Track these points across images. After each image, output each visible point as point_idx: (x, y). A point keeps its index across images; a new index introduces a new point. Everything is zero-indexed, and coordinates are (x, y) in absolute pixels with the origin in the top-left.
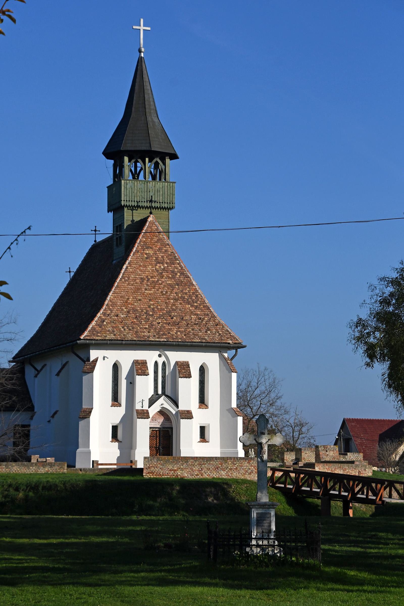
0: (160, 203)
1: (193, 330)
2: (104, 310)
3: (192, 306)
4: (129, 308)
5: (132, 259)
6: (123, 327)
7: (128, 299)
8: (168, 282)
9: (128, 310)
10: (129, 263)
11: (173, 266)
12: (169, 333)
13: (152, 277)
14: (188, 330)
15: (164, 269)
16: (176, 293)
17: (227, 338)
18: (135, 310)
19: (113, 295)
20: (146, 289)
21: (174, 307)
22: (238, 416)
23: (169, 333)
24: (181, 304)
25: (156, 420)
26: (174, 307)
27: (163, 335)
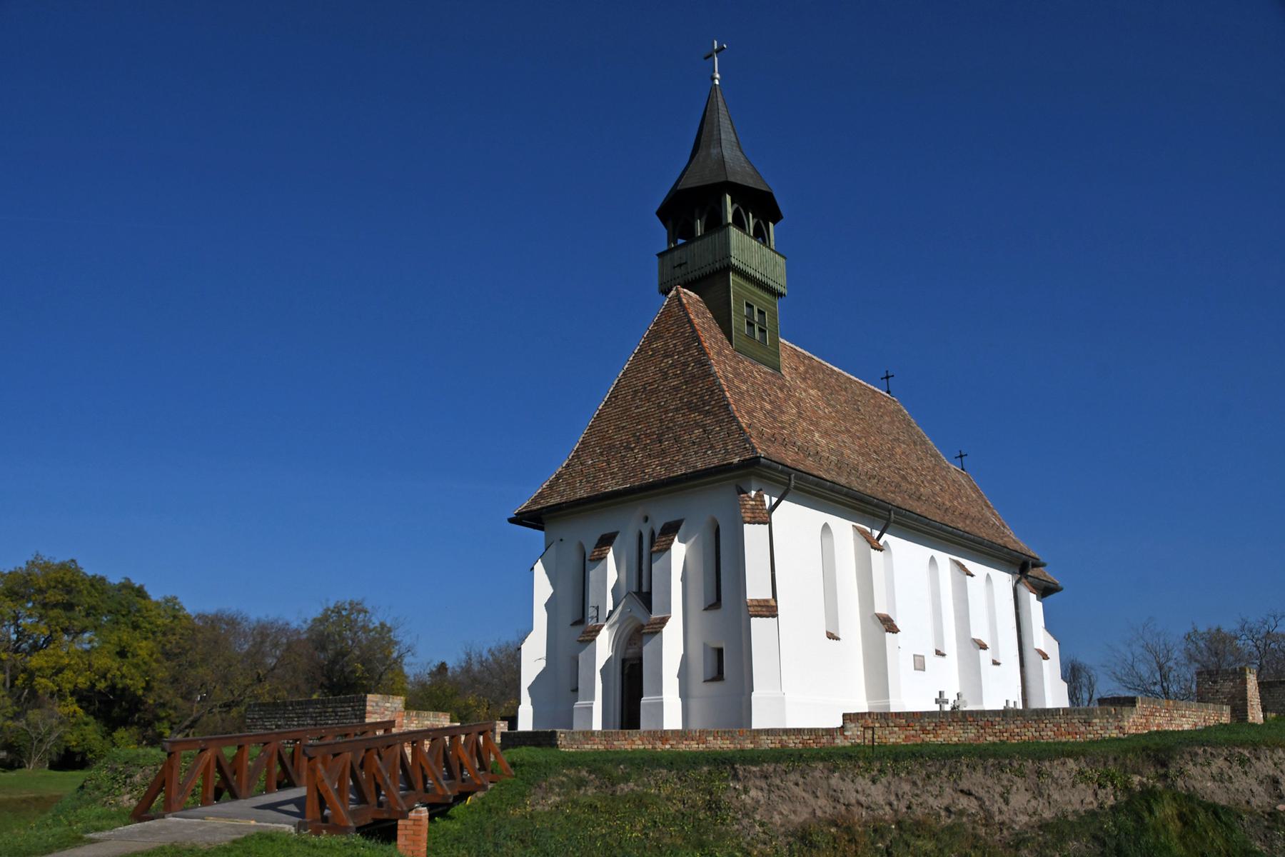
0: (709, 265)
1: (684, 456)
2: (570, 460)
4: (604, 447)
6: (581, 482)
8: (672, 384)
9: (602, 450)
10: (624, 374)
11: (687, 353)
12: (643, 472)
13: (651, 384)
14: (677, 458)
15: (671, 365)
17: (736, 454)
18: (611, 447)
19: (589, 431)
20: (637, 407)
21: (671, 425)
23: (643, 472)
24: (684, 415)
25: (635, 644)
26: (671, 425)
27: (631, 477)
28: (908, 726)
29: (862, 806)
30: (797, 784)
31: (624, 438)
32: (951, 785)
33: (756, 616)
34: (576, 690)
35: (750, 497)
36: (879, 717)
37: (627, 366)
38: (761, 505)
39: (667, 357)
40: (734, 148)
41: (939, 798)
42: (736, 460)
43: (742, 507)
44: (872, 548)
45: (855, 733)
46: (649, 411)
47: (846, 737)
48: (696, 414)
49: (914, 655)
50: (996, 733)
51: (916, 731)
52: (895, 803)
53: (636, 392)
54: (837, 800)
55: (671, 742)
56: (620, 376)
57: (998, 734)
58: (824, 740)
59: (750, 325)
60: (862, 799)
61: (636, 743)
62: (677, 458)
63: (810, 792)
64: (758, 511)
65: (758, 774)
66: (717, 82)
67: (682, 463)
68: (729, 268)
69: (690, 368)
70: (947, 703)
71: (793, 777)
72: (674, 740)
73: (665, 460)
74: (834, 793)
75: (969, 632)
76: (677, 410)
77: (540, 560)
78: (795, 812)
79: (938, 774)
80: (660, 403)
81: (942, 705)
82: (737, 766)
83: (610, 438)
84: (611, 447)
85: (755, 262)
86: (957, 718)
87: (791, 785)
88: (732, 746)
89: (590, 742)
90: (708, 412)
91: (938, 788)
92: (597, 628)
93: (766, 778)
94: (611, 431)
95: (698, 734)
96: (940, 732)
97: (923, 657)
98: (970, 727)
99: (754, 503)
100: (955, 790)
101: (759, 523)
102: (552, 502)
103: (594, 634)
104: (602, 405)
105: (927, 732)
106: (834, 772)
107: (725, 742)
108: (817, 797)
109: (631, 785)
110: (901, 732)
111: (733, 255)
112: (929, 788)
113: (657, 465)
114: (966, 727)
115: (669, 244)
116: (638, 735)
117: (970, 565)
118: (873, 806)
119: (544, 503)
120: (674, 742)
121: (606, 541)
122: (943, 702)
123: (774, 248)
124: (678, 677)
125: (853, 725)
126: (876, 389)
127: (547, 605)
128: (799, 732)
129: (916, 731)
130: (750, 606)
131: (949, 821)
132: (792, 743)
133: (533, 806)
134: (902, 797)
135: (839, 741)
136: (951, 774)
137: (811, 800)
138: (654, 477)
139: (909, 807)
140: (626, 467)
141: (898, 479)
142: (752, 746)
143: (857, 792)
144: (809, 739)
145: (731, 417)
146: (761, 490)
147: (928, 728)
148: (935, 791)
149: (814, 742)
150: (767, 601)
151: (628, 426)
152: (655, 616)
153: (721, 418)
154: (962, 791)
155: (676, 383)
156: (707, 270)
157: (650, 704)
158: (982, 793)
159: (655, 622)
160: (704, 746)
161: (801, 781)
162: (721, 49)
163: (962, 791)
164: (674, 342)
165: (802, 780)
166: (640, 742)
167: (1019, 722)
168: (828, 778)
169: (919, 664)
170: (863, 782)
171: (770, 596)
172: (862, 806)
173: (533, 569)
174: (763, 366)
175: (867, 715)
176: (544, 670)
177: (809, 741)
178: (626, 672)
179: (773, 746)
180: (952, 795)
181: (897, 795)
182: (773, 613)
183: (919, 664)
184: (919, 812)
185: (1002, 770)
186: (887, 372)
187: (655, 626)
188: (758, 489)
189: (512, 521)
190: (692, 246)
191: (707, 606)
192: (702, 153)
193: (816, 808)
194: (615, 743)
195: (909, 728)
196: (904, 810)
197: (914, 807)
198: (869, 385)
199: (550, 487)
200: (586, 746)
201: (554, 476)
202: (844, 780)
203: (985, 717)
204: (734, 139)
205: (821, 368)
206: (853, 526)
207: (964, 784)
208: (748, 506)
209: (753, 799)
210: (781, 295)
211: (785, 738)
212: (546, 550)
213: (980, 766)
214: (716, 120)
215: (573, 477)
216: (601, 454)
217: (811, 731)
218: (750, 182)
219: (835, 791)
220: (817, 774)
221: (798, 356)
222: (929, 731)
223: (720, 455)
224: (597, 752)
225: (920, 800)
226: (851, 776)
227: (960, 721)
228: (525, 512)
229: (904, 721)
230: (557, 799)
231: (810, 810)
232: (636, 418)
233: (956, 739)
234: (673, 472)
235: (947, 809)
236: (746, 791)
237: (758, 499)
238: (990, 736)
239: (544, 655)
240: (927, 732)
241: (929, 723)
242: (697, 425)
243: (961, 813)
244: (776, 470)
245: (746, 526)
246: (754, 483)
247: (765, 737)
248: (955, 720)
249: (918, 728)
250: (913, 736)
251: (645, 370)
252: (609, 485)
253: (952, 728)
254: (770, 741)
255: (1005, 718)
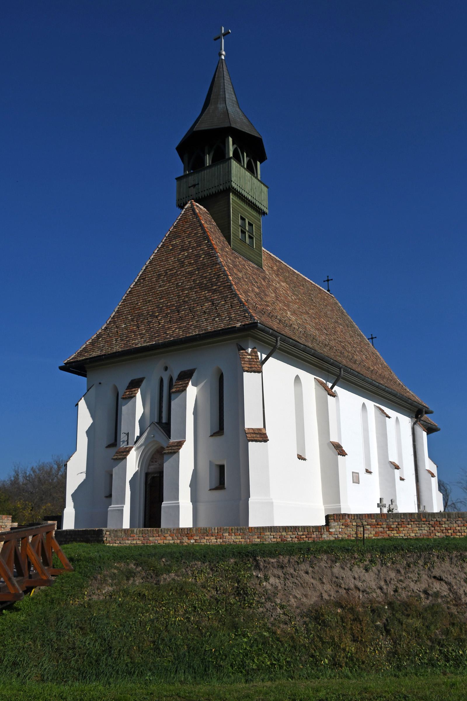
1: (197, 321)
3: (209, 291)
4: (134, 315)
5: (155, 257)
6: (116, 340)
7: (137, 303)
8: (188, 270)
9: (133, 317)
10: (150, 263)
11: (200, 248)
12: (165, 333)
13: (171, 270)
14: (192, 323)
15: (186, 257)
16: (194, 281)
17: (238, 321)
19: (123, 303)
20: (160, 287)
21: (187, 299)
22: (249, 441)
23: (165, 333)
24: (196, 292)
25: (156, 462)
26: (187, 299)
27: (156, 337)
28: (378, 525)
29: (359, 590)
30: (307, 573)
31: (150, 308)
32: (426, 573)
33: (252, 441)
34: (110, 496)
35: (247, 353)
36: (356, 518)
37: (152, 257)
38: (256, 359)
39: (184, 250)
40: (235, 105)
41: (418, 583)
42: (238, 325)
43: (242, 359)
44: (329, 394)
45: (338, 530)
46: (170, 289)
47: (331, 533)
48: (206, 292)
49: (353, 472)
50: (443, 530)
51: (383, 528)
52: (385, 587)
53: (160, 275)
54: (339, 586)
55: (195, 538)
56: (147, 264)
57: (444, 531)
58: (314, 536)
59: (243, 232)
60: (359, 584)
61: (168, 538)
62: (192, 323)
63: (317, 579)
64: (253, 363)
65: (275, 566)
66: (223, 57)
67: (196, 327)
68: (230, 189)
69: (201, 259)
70: (385, 506)
71: (304, 567)
72: (197, 536)
73: (182, 325)
74: (336, 580)
75: (387, 457)
76: (191, 289)
77: (83, 398)
78: (306, 596)
79: (415, 563)
80: (178, 283)
81: (382, 508)
82: (258, 558)
83: (139, 309)
84: (140, 315)
85: (248, 188)
86: (414, 518)
87: (302, 573)
88: (243, 540)
89: (130, 538)
90: (215, 290)
91: (417, 575)
92: (127, 449)
93: (282, 567)
94: (140, 304)
95: (216, 531)
96: (401, 529)
97: (358, 473)
98: (423, 526)
99: (250, 357)
100: (430, 577)
101: (255, 372)
102: (94, 354)
103: (125, 453)
104: (133, 284)
105: (392, 529)
106: (336, 562)
107: (237, 537)
108: (323, 583)
109: (173, 575)
110: (372, 529)
111: (233, 180)
112: (410, 575)
113: (176, 329)
114: (420, 526)
115: (185, 171)
116: (169, 533)
117: (388, 411)
118: (368, 590)
119: (87, 356)
120: (198, 538)
121: (135, 384)
122: (383, 506)
123: (260, 179)
124: (190, 486)
125: (336, 524)
126: (321, 288)
127: (88, 432)
128: (295, 528)
129: (383, 528)
130: (248, 433)
131: (428, 602)
132: (289, 537)
133: (90, 596)
134: (390, 582)
135: (326, 536)
136: (425, 564)
137: (319, 586)
138: (174, 337)
139: (396, 591)
140: (152, 330)
141: (341, 349)
142: (259, 540)
143: (355, 578)
144: (303, 535)
145: (233, 294)
146: (255, 348)
147: (392, 526)
148: (415, 577)
149: (306, 537)
150: (260, 429)
151: (153, 300)
152: (173, 440)
153: (225, 295)
154: (435, 577)
155: (190, 269)
156: (214, 191)
157: (168, 507)
158: (450, 579)
159: (174, 445)
160: (221, 540)
161: (310, 570)
162: (227, 34)
163: (435, 577)
164: (189, 240)
165: (311, 569)
166: (171, 538)
167: (460, 522)
168: (331, 567)
169: (356, 479)
170: (358, 571)
171: (262, 427)
172: (359, 590)
173: (77, 405)
174: (251, 263)
175: (347, 516)
176: (85, 480)
177: (302, 537)
178: (149, 483)
179: (275, 540)
180: (427, 580)
181: (385, 581)
182: (265, 439)
183: (356, 479)
184: (404, 595)
185: (464, 560)
186: (328, 277)
187: (173, 448)
188: (253, 347)
189: (61, 368)
190: (203, 172)
191: (212, 434)
192: (211, 107)
193: (323, 592)
194: (151, 539)
195: (378, 526)
196: (392, 593)
197: (400, 590)
198: (316, 285)
199: (92, 344)
200: (127, 541)
201: (95, 336)
202: (344, 569)
203: (434, 518)
204: (234, 99)
205: (289, 271)
206: (315, 378)
207: (437, 572)
208: (246, 359)
209: (272, 585)
210: (264, 213)
211: (284, 534)
212: (88, 391)
213: (447, 557)
214: (222, 84)
215: (110, 337)
216: (132, 320)
217: (304, 528)
218: (246, 129)
219: (337, 578)
220: (323, 564)
221: (272, 260)
222: (393, 528)
223: (225, 321)
224: (136, 547)
225: (404, 585)
226: (349, 565)
227: (416, 521)
228: (72, 362)
229: (374, 520)
230: (110, 588)
231: (318, 594)
232: (159, 294)
233: (413, 535)
234: (189, 333)
235: (425, 592)
236: (266, 579)
237: (254, 354)
238: (438, 532)
239: (84, 469)
240: (392, 529)
241: (393, 522)
242: (207, 300)
243: (437, 595)
244: (267, 333)
245: (245, 374)
246: (251, 343)
247: (269, 533)
248: (413, 520)
249: (385, 526)
250: (381, 532)
251: (167, 260)
252: (139, 343)
253: (410, 526)
254: (272, 537)
255: (449, 519)
